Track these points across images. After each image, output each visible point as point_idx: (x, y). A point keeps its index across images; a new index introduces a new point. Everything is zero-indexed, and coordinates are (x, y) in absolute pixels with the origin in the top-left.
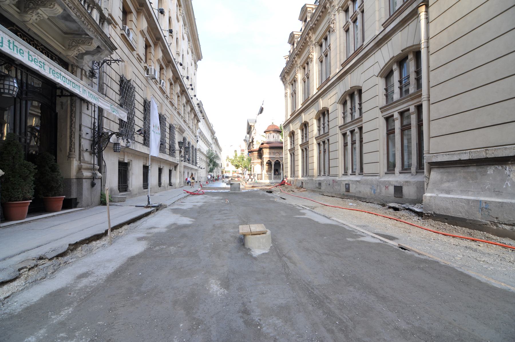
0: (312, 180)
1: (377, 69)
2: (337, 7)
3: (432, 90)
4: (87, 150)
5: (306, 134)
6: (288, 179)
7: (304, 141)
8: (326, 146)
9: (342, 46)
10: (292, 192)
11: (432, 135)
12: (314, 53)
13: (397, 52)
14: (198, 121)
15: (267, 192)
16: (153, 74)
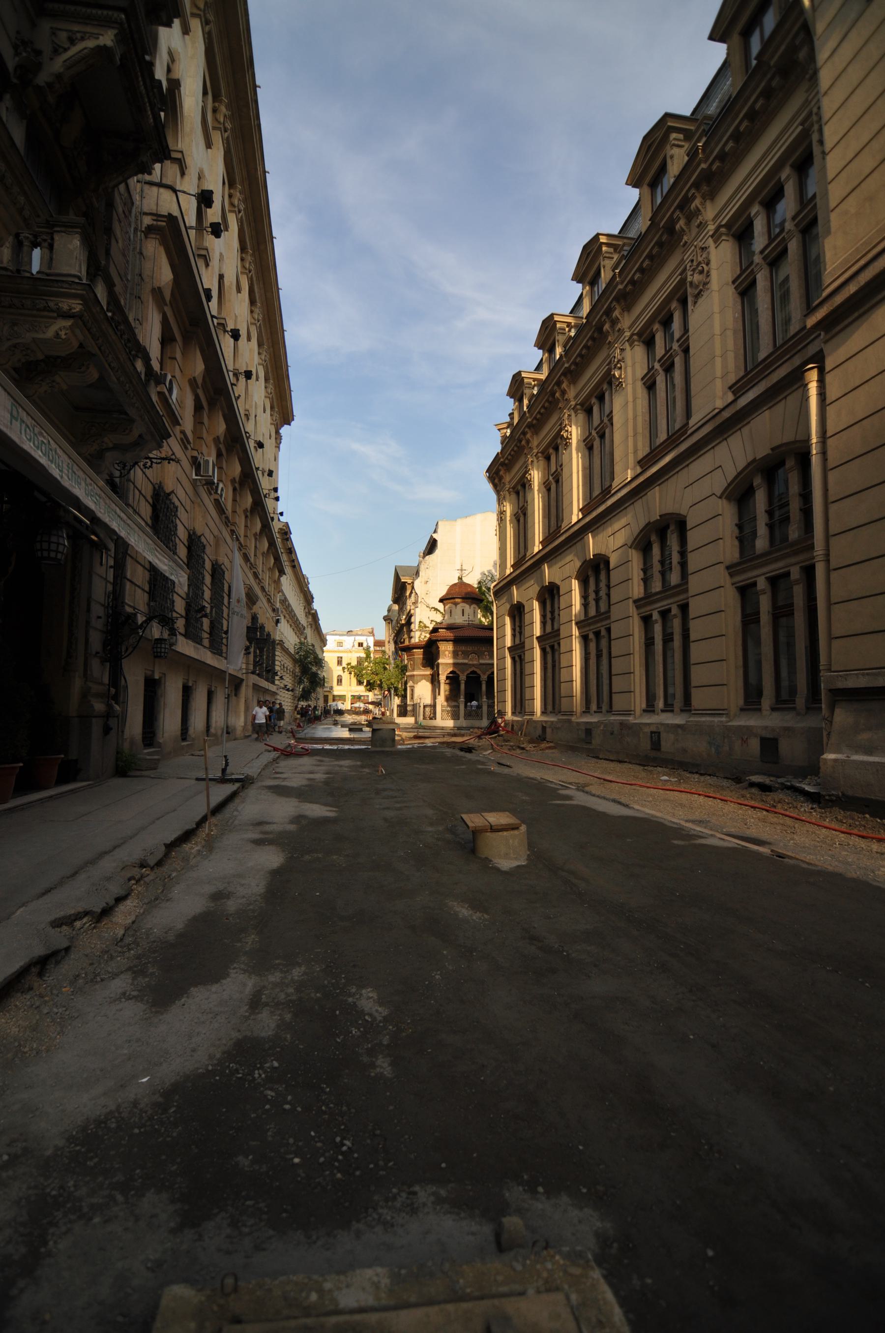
0: (570, 721)
1: (719, 483)
2: (628, 334)
3: (832, 541)
4: (97, 653)
5: (552, 612)
6: (506, 718)
7: (549, 629)
8: (604, 643)
9: (640, 419)
10: (519, 751)
11: (836, 632)
12: (574, 427)
13: (763, 451)
14: (282, 572)
15: (462, 749)
16: (210, 473)
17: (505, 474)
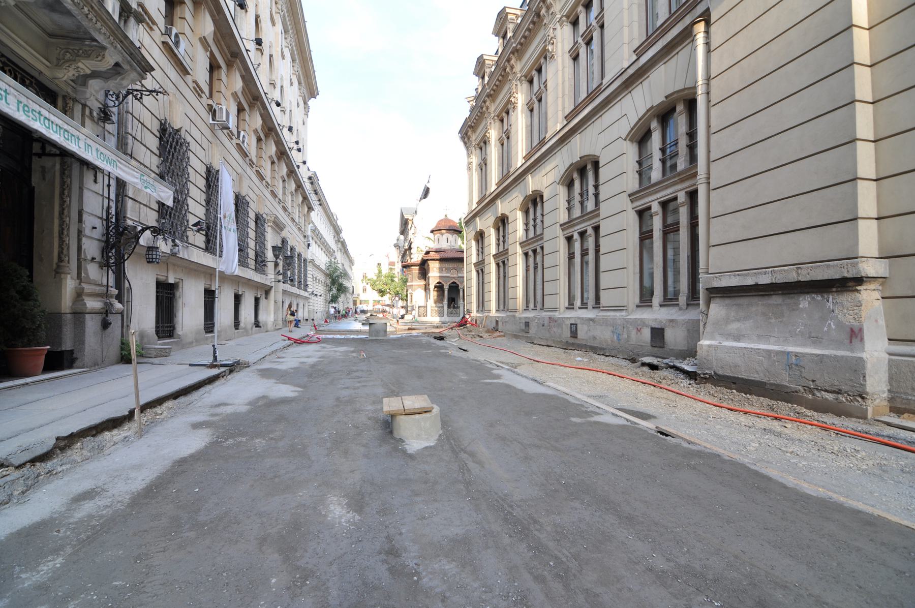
0: (514, 316)
1: (625, 127)
2: (559, 16)
3: (713, 165)
4: (93, 259)
5: (504, 237)
7: (501, 249)
8: (539, 258)
9: (567, 84)
10: (478, 339)
11: (712, 243)
13: (659, 99)
14: (310, 209)
15: (435, 338)
16: (224, 119)
17: (471, 132)
